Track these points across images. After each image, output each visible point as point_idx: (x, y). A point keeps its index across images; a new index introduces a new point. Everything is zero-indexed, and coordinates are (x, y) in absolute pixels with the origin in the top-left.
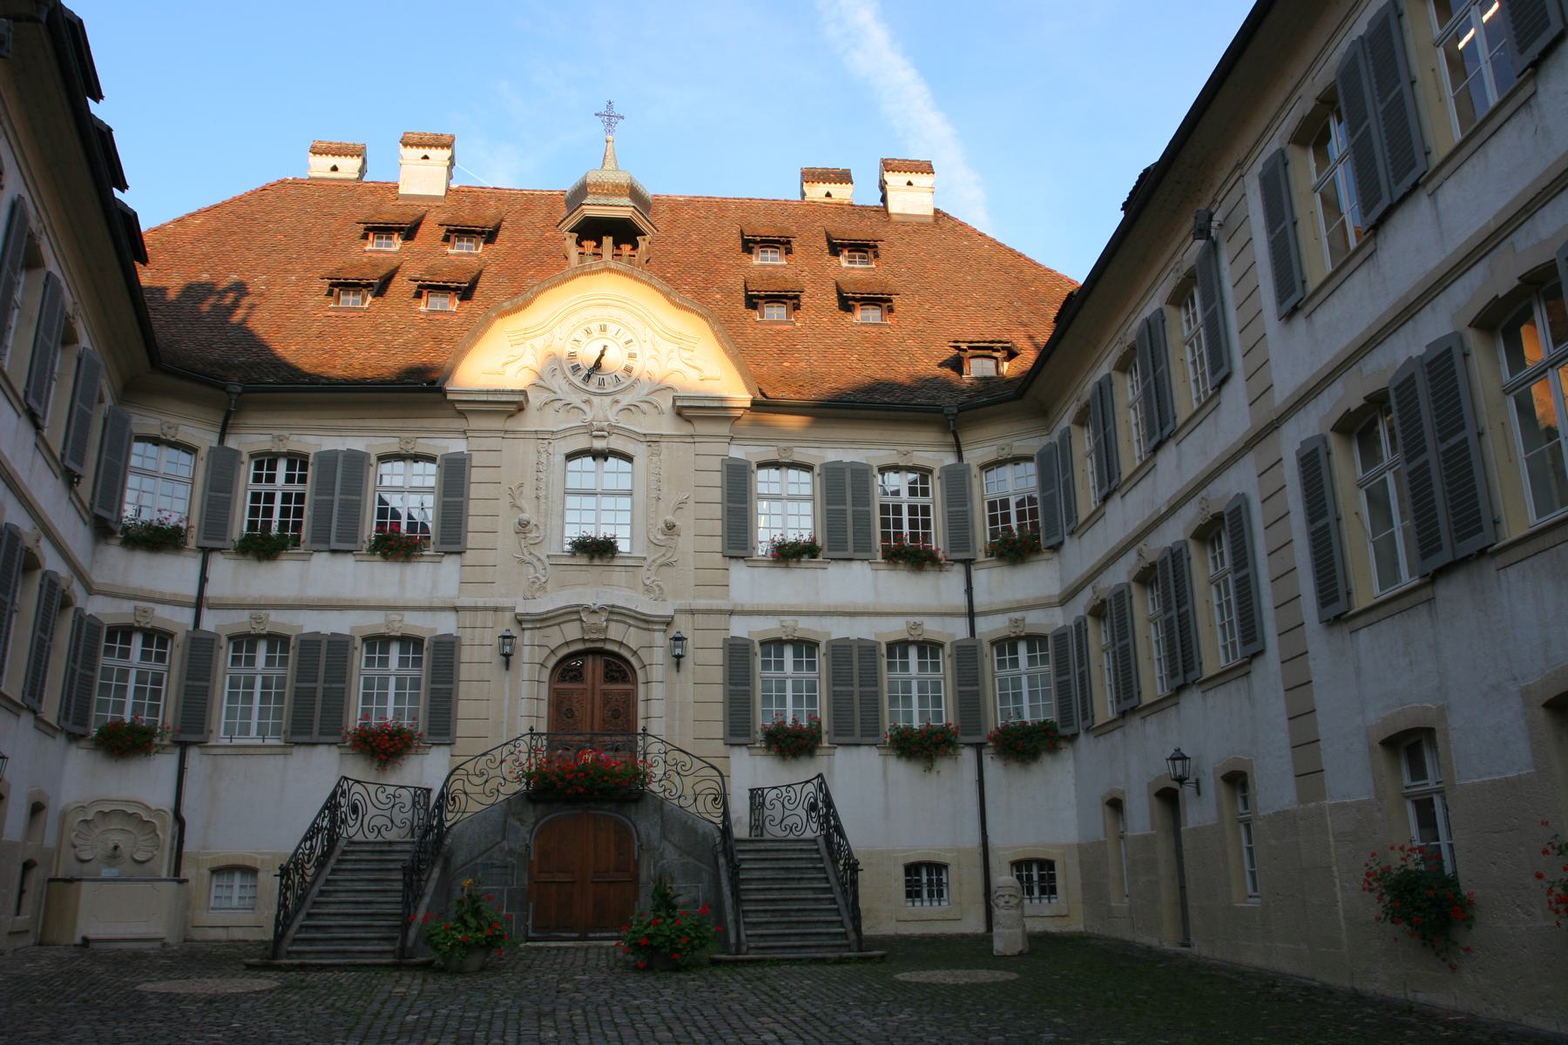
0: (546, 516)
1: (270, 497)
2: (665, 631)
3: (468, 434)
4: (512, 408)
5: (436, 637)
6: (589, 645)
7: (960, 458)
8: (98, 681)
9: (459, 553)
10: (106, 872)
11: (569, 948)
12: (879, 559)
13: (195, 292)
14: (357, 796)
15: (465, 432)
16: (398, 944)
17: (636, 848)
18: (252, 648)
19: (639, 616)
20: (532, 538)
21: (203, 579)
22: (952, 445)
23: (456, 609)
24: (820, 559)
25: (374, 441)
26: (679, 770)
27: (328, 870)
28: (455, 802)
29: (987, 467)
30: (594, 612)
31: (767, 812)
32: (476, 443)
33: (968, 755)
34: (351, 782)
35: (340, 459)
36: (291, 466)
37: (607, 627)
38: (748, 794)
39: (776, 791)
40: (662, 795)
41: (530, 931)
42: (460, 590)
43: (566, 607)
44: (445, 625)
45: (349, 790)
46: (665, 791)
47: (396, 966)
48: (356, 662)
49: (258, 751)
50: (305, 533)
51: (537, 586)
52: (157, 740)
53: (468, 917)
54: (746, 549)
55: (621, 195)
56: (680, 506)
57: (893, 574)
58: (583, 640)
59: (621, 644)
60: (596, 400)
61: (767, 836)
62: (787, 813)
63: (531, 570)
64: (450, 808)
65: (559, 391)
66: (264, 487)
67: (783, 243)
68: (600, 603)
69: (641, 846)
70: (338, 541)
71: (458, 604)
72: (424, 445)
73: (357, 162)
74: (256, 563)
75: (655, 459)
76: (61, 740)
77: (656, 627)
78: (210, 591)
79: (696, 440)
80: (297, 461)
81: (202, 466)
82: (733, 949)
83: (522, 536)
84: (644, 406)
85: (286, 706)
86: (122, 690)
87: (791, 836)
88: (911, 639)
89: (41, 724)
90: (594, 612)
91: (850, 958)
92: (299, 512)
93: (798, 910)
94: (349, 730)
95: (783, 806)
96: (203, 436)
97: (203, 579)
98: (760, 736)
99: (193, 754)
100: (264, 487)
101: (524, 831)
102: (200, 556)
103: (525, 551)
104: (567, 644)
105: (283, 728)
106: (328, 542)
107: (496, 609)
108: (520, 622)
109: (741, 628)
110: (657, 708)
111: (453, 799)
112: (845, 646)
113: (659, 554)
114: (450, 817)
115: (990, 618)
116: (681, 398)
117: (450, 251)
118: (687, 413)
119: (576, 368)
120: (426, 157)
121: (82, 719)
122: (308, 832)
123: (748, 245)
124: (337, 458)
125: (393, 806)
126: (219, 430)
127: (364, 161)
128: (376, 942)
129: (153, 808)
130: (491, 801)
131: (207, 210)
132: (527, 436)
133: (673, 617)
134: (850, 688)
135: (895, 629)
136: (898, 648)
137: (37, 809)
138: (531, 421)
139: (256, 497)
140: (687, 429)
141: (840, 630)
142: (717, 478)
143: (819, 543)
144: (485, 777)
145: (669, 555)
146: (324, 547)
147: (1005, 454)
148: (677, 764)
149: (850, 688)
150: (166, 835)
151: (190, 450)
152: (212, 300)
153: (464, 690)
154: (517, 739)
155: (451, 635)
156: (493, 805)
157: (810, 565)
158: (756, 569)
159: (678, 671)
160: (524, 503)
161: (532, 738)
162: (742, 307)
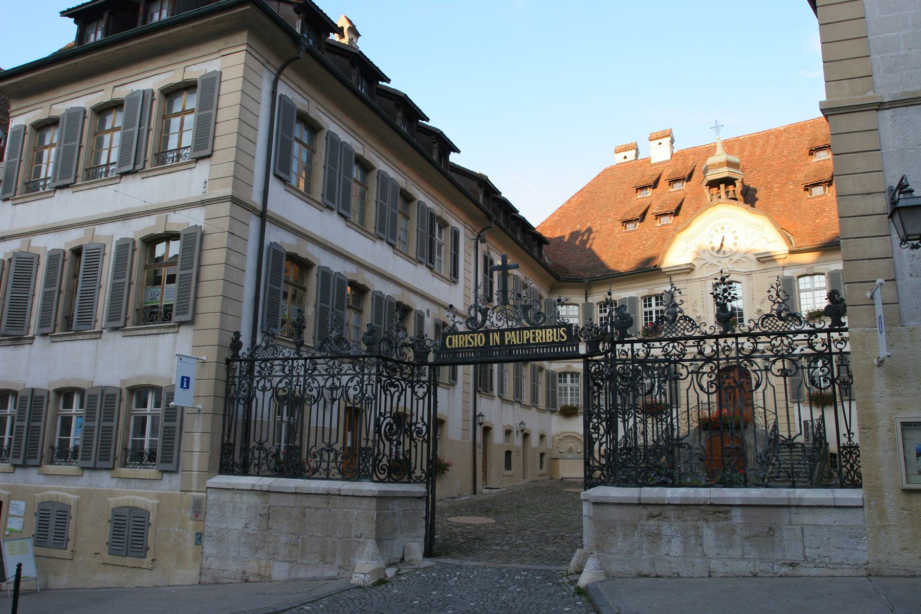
4: (688, 270)
8: (558, 392)
10: (569, 456)
13: (574, 235)
35: (627, 300)
52: (579, 411)
55: (723, 167)
60: (722, 260)
67: (827, 147)
73: (634, 152)
76: (548, 414)
81: (581, 310)
86: (566, 394)
89: (539, 410)
96: (580, 300)
117: (672, 190)
118: (761, 260)
119: (713, 248)
120: (660, 144)
121: (554, 405)
123: (812, 152)
127: (637, 150)
131: (578, 193)
137: (542, 437)
138: (697, 274)
140: (763, 266)
152: (580, 239)
160: (697, 309)
162: (802, 191)
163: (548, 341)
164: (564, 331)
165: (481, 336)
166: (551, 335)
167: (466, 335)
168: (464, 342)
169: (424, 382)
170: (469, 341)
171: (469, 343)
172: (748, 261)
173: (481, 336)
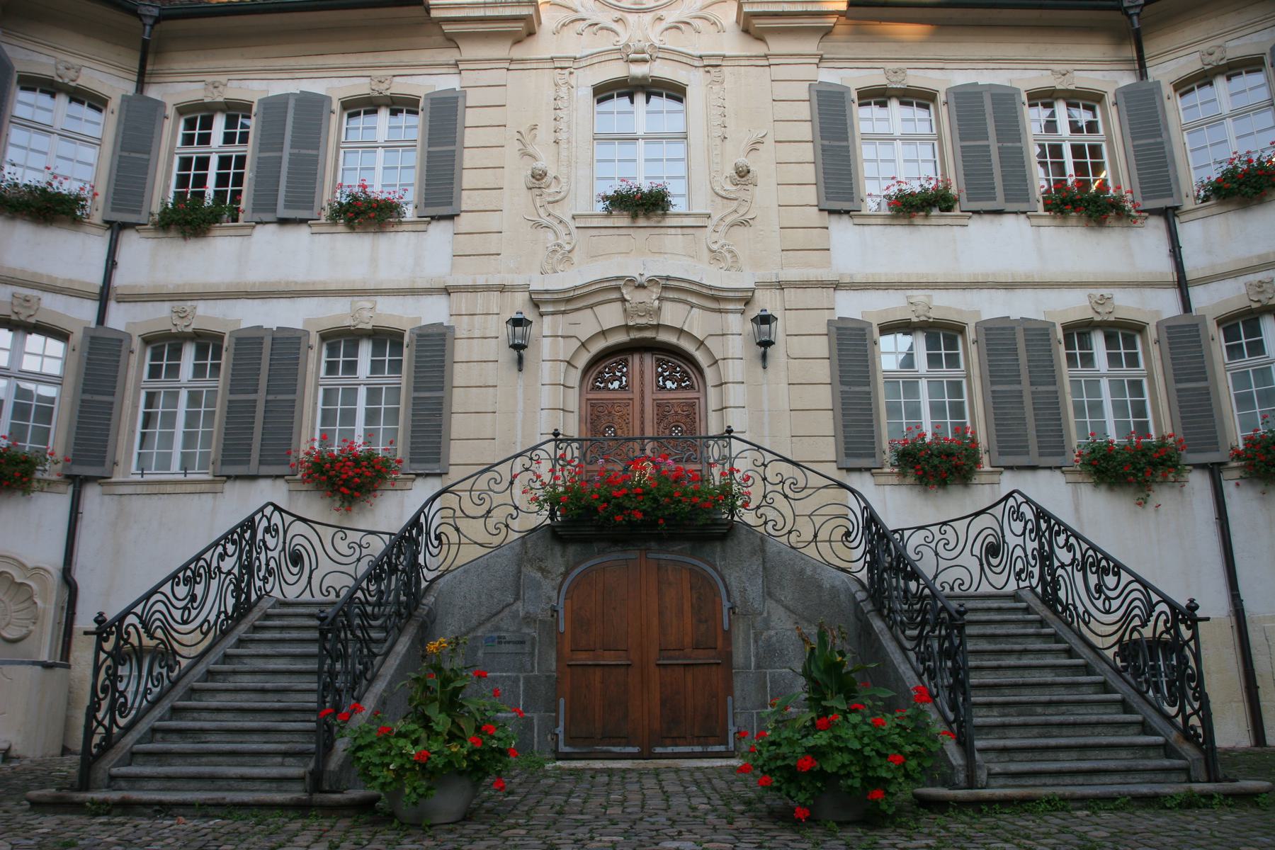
0: (569, 165)
1: (203, 163)
2: (743, 313)
3: (461, 67)
4: (519, 26)
5: (420, 328)
6: (635, 335)
7: (1142, 73)
9: (451, 217)
11: (625, 771)
12: (1041, 211)
14: (297, 540)
15: (456, 65)
16: (312, 765)
17: (725, 611)
18: (176, 353)
19: (705, 291)
20: (549, 194)
21: (111, 264)
22: (1130, 61)
23: (447, 291)
24: (957, 212)
25: (336, 83)
26: (788, 491)
27: (232, 639)
28: (441, 543)
29: (1184, 86)
30: (641, 286)
32: (470, 78)
33: (1199, 483)
34: (288, 519)
35: (292, 104)
36: (231, 122)
37: (659, 308)
39: (923, 533)
40: (761, 529)
41: (561, 744)
42: (453, 266)
43: (601, 281)
44: (433, 312)
45: (285, 532)
46: (766, 523)
47: (300, 809)
48: (311, 366)
49: (179, 489)
50: (245, 203)
51: (559, 256)
53: (433, 711)
54: (851, 200)
56: (754, 147)
57: (1063, 230)
58: (627, 328)
59: (681, 332)
60: (631, 18)
62: (943, 564)
63: (551, 236)
64: (435, 551)
65: (580, 9)
66: (195, 151)
68: (648, 274)
69: (732, 608)
70: (286, 207)
71: (451, 281)
72: (403, 86)
74: (180, 242)
75: (716, 88)
77: (731, 306)
78: (121, 280)
79: (772, 61)
80: (236, 111)
82: (961, 777)
83: (537, 192)
84: (697, 23)
85: (215, 429)
88: (1098, 318)
90: (641, 286)
91: (1209, 796)
92: (239, 179)
93: (1049, 703)
94: (302, 455)
95: (937, 554)
97: (111, 264)
98: (889, 457)
99: (92, 494)
100: (195, 151)
101: (548, 587)
102: (108, 234)
103: (541, 211)
104: (604, 333)
105: (212, 457)
106: (275, 211)
107: (502, 289)
108: (536, 305)
109: (850, 306)
111: (438, 537)
112: (1003, 329)
113: (730, 210)
114: (431, 561)
115: (1214, 286)
122: (185, 567)
124: (287, 103)
125: (359, 560)
126: (135, 78)
128: (279, 759)
129: (30, 564)
130: (496, 541)
132: (541, 65)
133: (753, 291)
134: (1017, 387)
135: (1074, 305)
136: (1078, 332)
139: (185, 163)
140: (758, 49)
141: (992, 307)
142: (804, 111)
143: (953, 190)
144: (485, 507)
145: (741, 212)
146: (266, 217)
147: (1214, 60)
148: (783, 482)
149: (1017, 387)
150: (49, 603)
151: (97, 102)
153: (459, 399)
154: (534, 448)
155: (442, 324)
156: (499, 547)
157: (943, 221)
158: (866, 228)
159: (765, 367)
161: (557, 446)
172: (713, 28)
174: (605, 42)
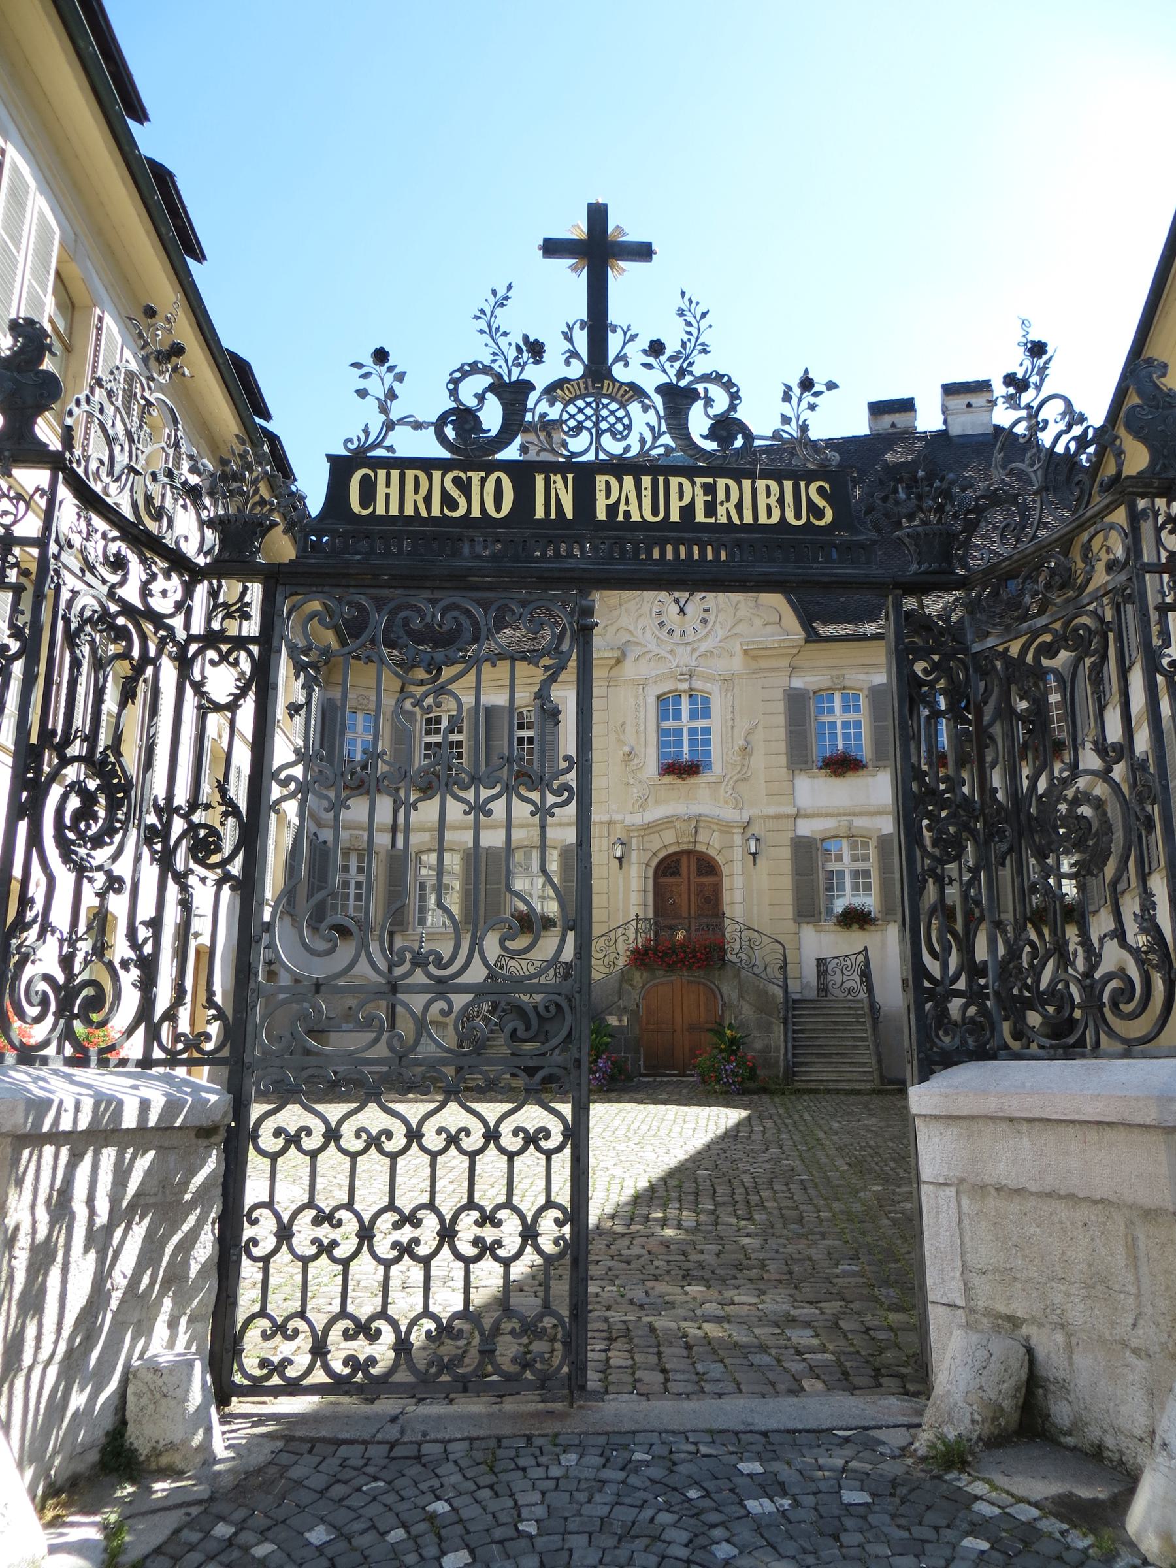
31: (829, 978)
38: (815, 963)
39: (836, 961)
61: (830, 997)
62: (846, 978)
86: (346, 896)
87: (849, 997)
93: (837, 1054)
109: (806, 828)
110: (738, 896)
116: (748, 643)
118: (751, 653)
130: (607, 971)
142: (780, 706)
163: (763, 519)
164: (820, 491)
165: (499, 482)
166: (773, 501)
167: (436, 475)
168: (428, 500)
169: (240, 642)
170: (445, 495)
171: (449, 502)
173: (499, 483)
174: (662, 669)
